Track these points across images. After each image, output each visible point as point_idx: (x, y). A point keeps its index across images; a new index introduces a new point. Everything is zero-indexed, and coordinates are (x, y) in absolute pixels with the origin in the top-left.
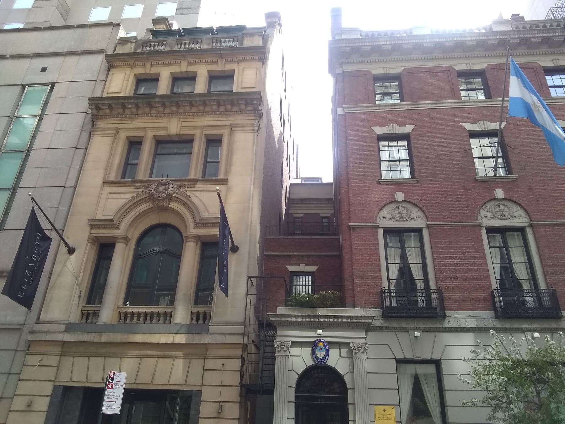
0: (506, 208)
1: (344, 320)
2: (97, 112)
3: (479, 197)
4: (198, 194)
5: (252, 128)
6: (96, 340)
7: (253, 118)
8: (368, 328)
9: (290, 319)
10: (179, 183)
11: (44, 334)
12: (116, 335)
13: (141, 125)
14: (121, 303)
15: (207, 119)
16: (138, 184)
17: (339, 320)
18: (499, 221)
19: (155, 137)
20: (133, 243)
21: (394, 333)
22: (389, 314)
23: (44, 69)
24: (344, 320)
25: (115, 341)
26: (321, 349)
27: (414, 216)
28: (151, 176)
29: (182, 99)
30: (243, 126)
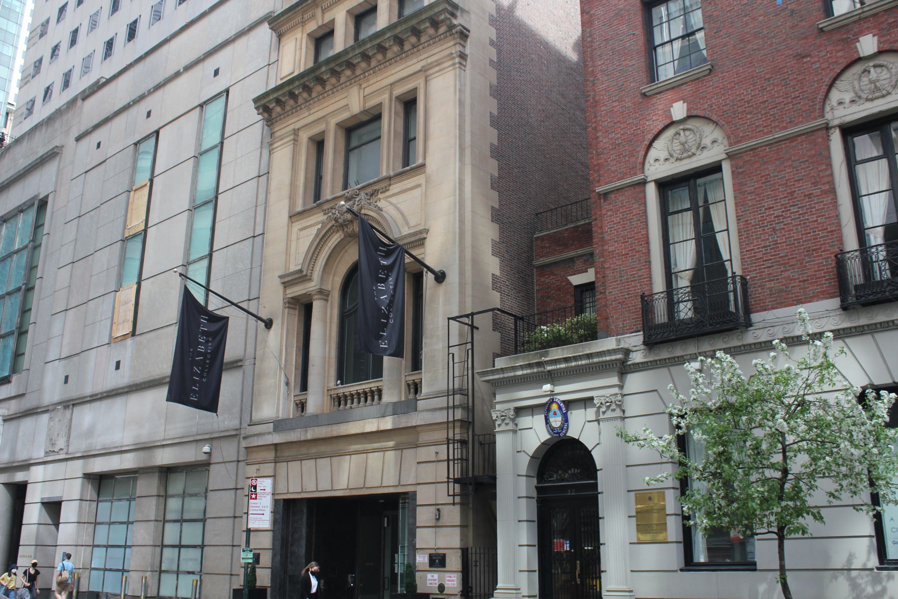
0: (885, 71)
1: (580, 363)
2: (270, 116)
3: (824, 66)
4: (393, 200)
5: (450, 63)
6: (303, 438)
7: (452, 43)
8: (623, 368)
9: (506, 375)
10: (369, 190)
11: (256, 438)
12: (320, 428)
13: (320, 114)
14: (332, 385)
15: (393, 71)
16: (326, 207)
17: (573, 364)
18: (868, 105)
19: (339, 125)
20: (336, 296)
21: (666, 369)
22: (656, 337)
23: (216, 73)
24: (580, 363)
25: (321, 436)
26: (555, 413)
27: (707, 141)
28: (345, 186)
29: (350, 55)
30: (438, 63)
